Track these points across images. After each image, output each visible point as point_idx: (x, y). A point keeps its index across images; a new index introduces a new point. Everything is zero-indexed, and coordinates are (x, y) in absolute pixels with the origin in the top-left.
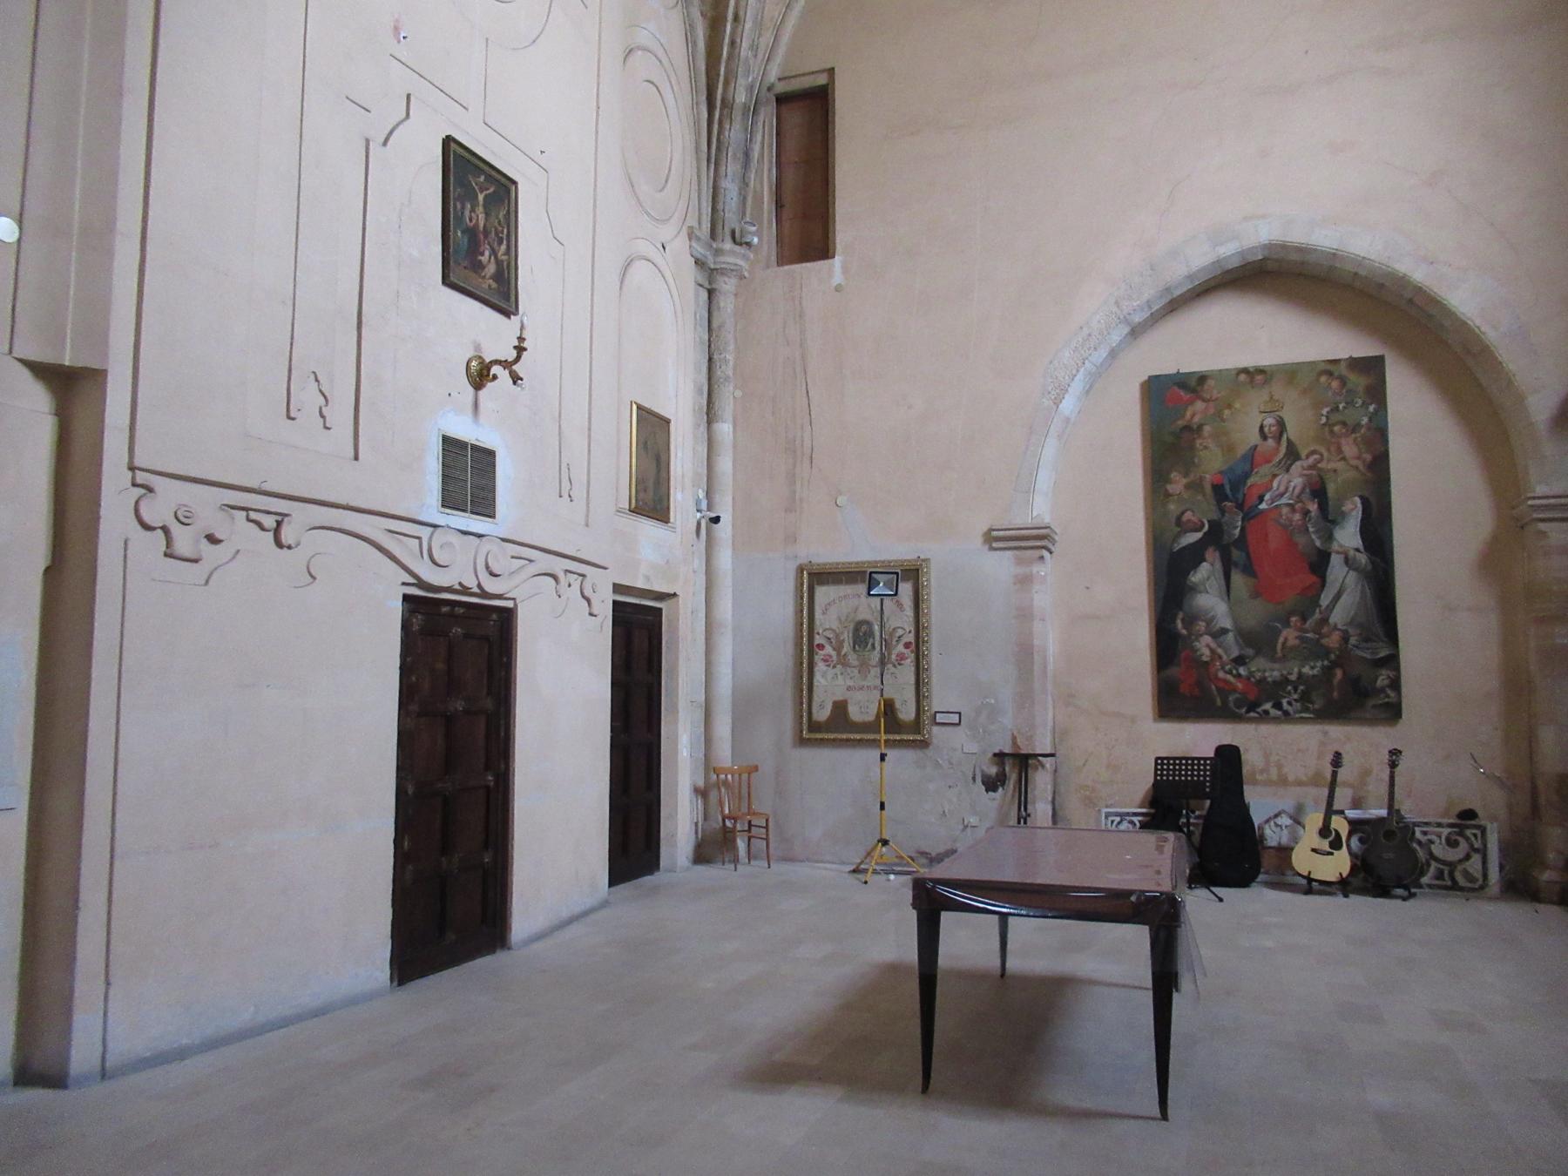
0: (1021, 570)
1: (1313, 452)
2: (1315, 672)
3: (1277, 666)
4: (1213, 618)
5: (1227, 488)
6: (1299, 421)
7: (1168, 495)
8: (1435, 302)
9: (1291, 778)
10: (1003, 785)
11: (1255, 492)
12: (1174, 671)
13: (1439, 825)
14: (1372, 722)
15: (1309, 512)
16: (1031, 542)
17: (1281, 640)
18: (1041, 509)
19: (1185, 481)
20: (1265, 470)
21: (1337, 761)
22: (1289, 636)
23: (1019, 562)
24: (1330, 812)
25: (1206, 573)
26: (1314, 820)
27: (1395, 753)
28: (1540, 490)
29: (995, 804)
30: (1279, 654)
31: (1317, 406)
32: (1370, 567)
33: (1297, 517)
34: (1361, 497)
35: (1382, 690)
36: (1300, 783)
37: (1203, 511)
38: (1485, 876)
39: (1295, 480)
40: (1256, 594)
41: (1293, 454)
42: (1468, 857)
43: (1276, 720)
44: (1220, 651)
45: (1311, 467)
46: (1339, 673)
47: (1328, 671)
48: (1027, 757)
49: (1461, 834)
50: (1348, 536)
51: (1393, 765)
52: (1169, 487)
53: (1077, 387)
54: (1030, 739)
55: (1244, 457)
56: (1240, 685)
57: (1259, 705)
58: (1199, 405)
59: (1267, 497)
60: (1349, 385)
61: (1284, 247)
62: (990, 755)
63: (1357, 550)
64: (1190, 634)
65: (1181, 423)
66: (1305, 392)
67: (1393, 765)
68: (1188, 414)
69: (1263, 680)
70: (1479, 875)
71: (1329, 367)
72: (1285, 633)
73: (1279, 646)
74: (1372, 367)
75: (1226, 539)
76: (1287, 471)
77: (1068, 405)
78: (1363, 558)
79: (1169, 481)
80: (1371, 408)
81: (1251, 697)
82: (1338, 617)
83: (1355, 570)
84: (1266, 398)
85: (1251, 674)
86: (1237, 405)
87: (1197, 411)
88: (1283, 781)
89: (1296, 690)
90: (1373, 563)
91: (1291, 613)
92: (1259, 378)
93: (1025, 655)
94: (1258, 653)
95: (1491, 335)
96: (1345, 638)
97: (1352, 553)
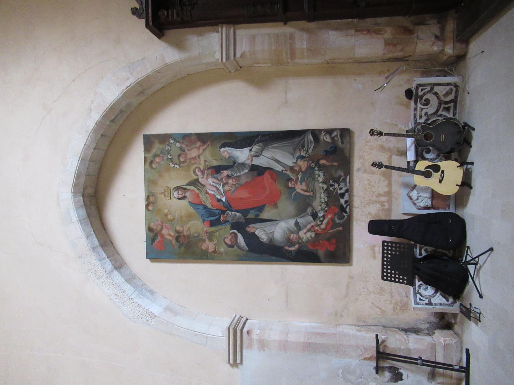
0: (255, 346)
1: (194, 172)
2: (321, 174)
3: (318, 195)
4: (289, 230)
5: (213, 218)
6: (176, 179)
7: (215, 251)
8: (112, 108)
9: (386, 189)
10: (398, 369)
11: (216, 203)
12: (321, 253)
13: (415, 109)
14: (351, 144)
15: (228, 176)
16: (238, 337)
17: (302, 192)
18: (218, 329)
20: (203, 198)
21: (379, 165)
22: (300, 188)
23: (250, 346)
24: (410, 170)
25: (261, 232)
26: (419, 180)
27: (372, 132)
28: (218, 56)
29: (411, 375)
30: (311, 194)
31: (168, 169)
32: (261, 144)
33: (231, 181)
34: (221, 148)
35: (332, 139)
36: (390, 185)
37: (225, 232)
38: (449, 84)
39: (209, 182)
40: (275, 205)
41: (195, 183)
42: (436, 94)
43: (351, 196)
44: (309, 227)
45: (203, 173)
46: (322, 162)
47: (321, 168)
48: (378, 352)
49: (421, 97)
50: (243, 155)
51: (380, 134)
52: (210, 251)
53: (145, 303)
54: (366, 349)
55: (195, 209)
56: (330, 216)
58: (165, 232)
59: (219, 197)
60: (159, 152)
61: (76, 185)
62: (377, 376)
63: (250, 150)
64: (298, 243)
65: (174, 242)
66: (161, 176)
67: (380, 134)
68: (170, 238)
69: (327, 203)
70: (448, 88)
71: (148, 162)
72: (298, 190)
73: (306, 193)
74: (149, 141)
75: (243, 220)
76: (204, 186)
77: (156, 309)
78: (255, 148)
79: (207, 249)
80: (172, 141)
81: (337, 210)
82: (289, 161)
83: (262, 151)
84: (163, 195)
85: (322, 209)
86: (166, 211)
87: (168, 233)
88: (389, 194)
89: (332, 185)
90: (258, 142)
92: (151, 199)
93: (309, 348)
94: (310, 205)
95: (132, 81)
96: (303, 158)
97: (252, 153)
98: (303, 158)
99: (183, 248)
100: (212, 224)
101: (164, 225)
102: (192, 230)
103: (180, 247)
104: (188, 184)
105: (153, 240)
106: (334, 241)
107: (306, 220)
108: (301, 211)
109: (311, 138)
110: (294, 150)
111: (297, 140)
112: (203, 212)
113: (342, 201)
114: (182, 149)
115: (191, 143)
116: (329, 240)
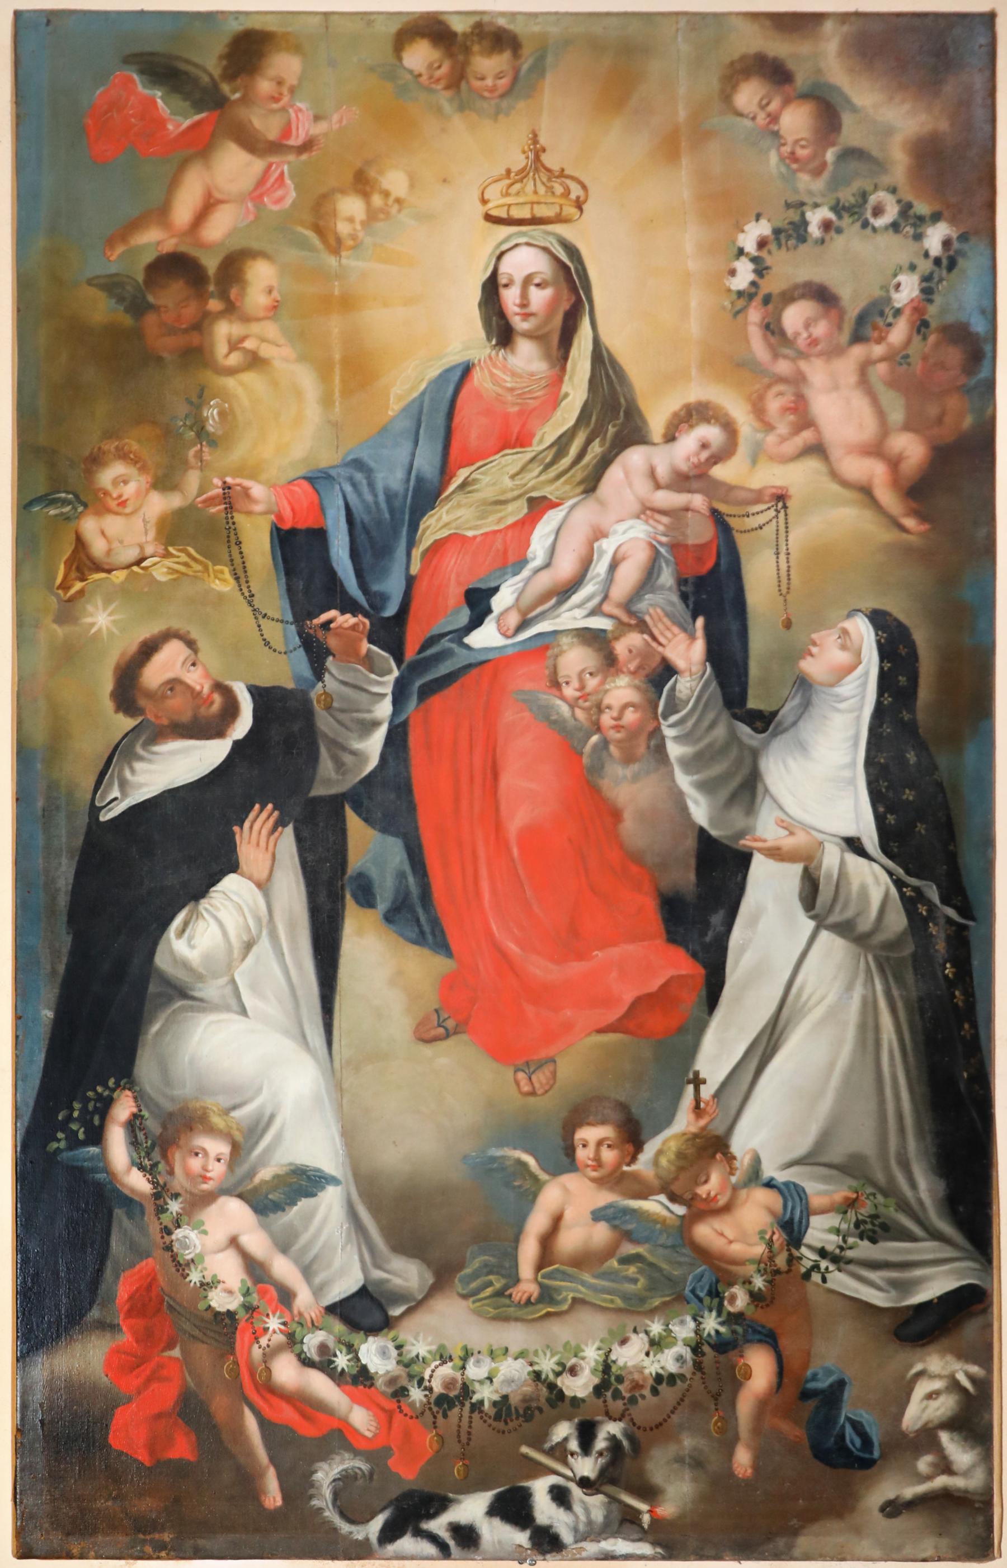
1: (695, 414)
2: (667, 1361)
3: (515, 1336)
4: (258, 1128)
7: (83, 562)
11: (456, 575)
15: (667, 671)
17: (537, 1223)
19: (159, 504)
20: (500, 474)
22: (571, 1206)
25: (235, 928)
30: (527, 1287)
31: (724, 206)
32: (897, 921)
33: (622, 691)
34: (878, 619)
35: (926, 1439)
37: (233, 643)
41: (614, 418)
45: (682, 481)
46: (760, 1367)
47: (716, 1362)
50: (820, 784)
52: (89, 526)
55: (416, 414)
56: (361, 1419)
57: (439, 1504)
58: (233, 167)
59: (500, 602)
60: (852, 133)
63: (854, 845)
64: (161, 1193)
65: (153, 240)
68: (184, 208)
69: (457, 1397)
71: (778, 47)
72: (552, 1196)
73: (528, 1251)
75: (329, 779)
76: (591, 484)
78: (872, 881)
81: (408, 1474)
82: (769, 1130)
83: (845, 929)
86: (394, 181)
87: (220, 195)
89: (587, 1433)
90: (911, 901)
91: (576, 1117)
92: (488, 66)
94: (443, 1276)
96: (792, 1230)
97: (832, 858)
98: (792, 1230)
99: (102, 310)
100: (298, 548)
101: (285, 165)
102: (244, 389)
103: (112, 285)
104: (600, 356)
105: (166, 71)
106: (182, 1448)
107: (334, 1251)
108: (403, 1214)
109: (936, 1285)
110: (851, 1168)
111: (925, 1188)
112: (392, 477)
113: (472, 1508)
114: (867, 324)
115: (914, 385)
116: (192, 1410)
